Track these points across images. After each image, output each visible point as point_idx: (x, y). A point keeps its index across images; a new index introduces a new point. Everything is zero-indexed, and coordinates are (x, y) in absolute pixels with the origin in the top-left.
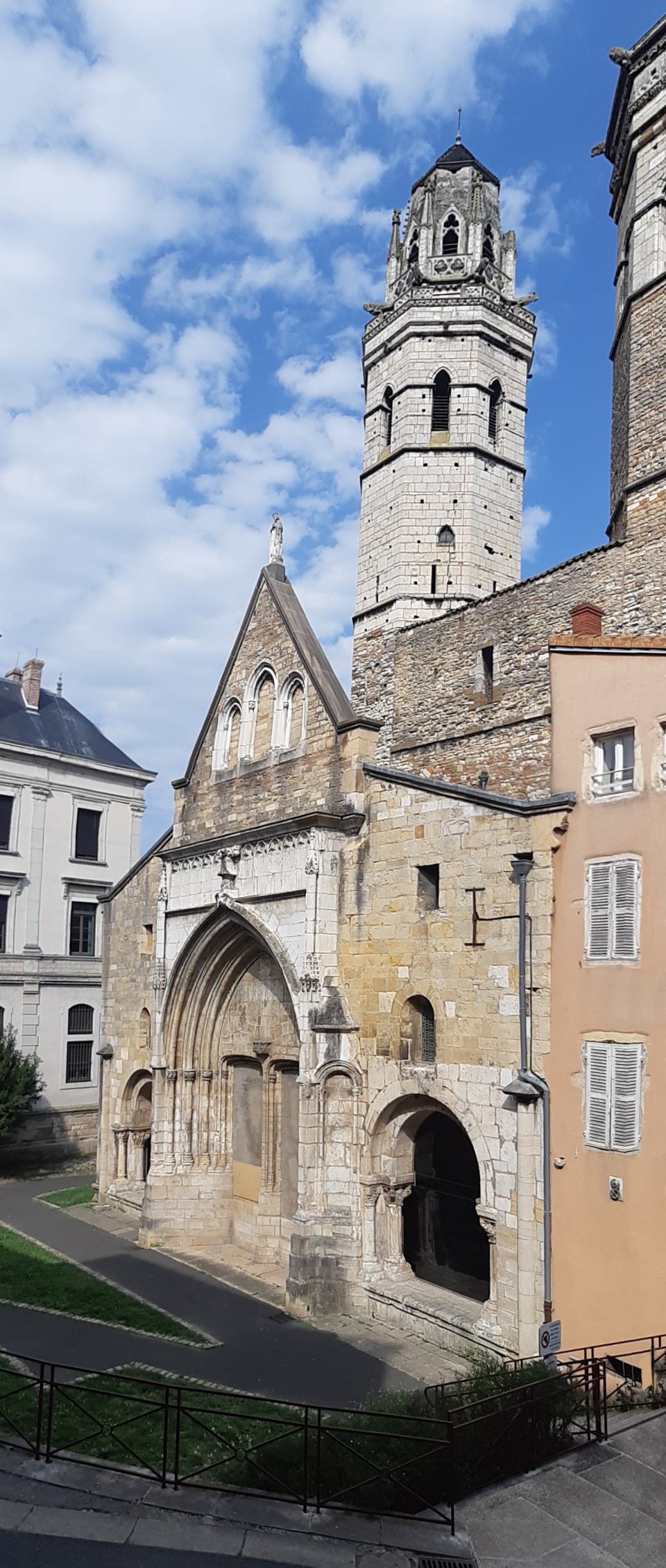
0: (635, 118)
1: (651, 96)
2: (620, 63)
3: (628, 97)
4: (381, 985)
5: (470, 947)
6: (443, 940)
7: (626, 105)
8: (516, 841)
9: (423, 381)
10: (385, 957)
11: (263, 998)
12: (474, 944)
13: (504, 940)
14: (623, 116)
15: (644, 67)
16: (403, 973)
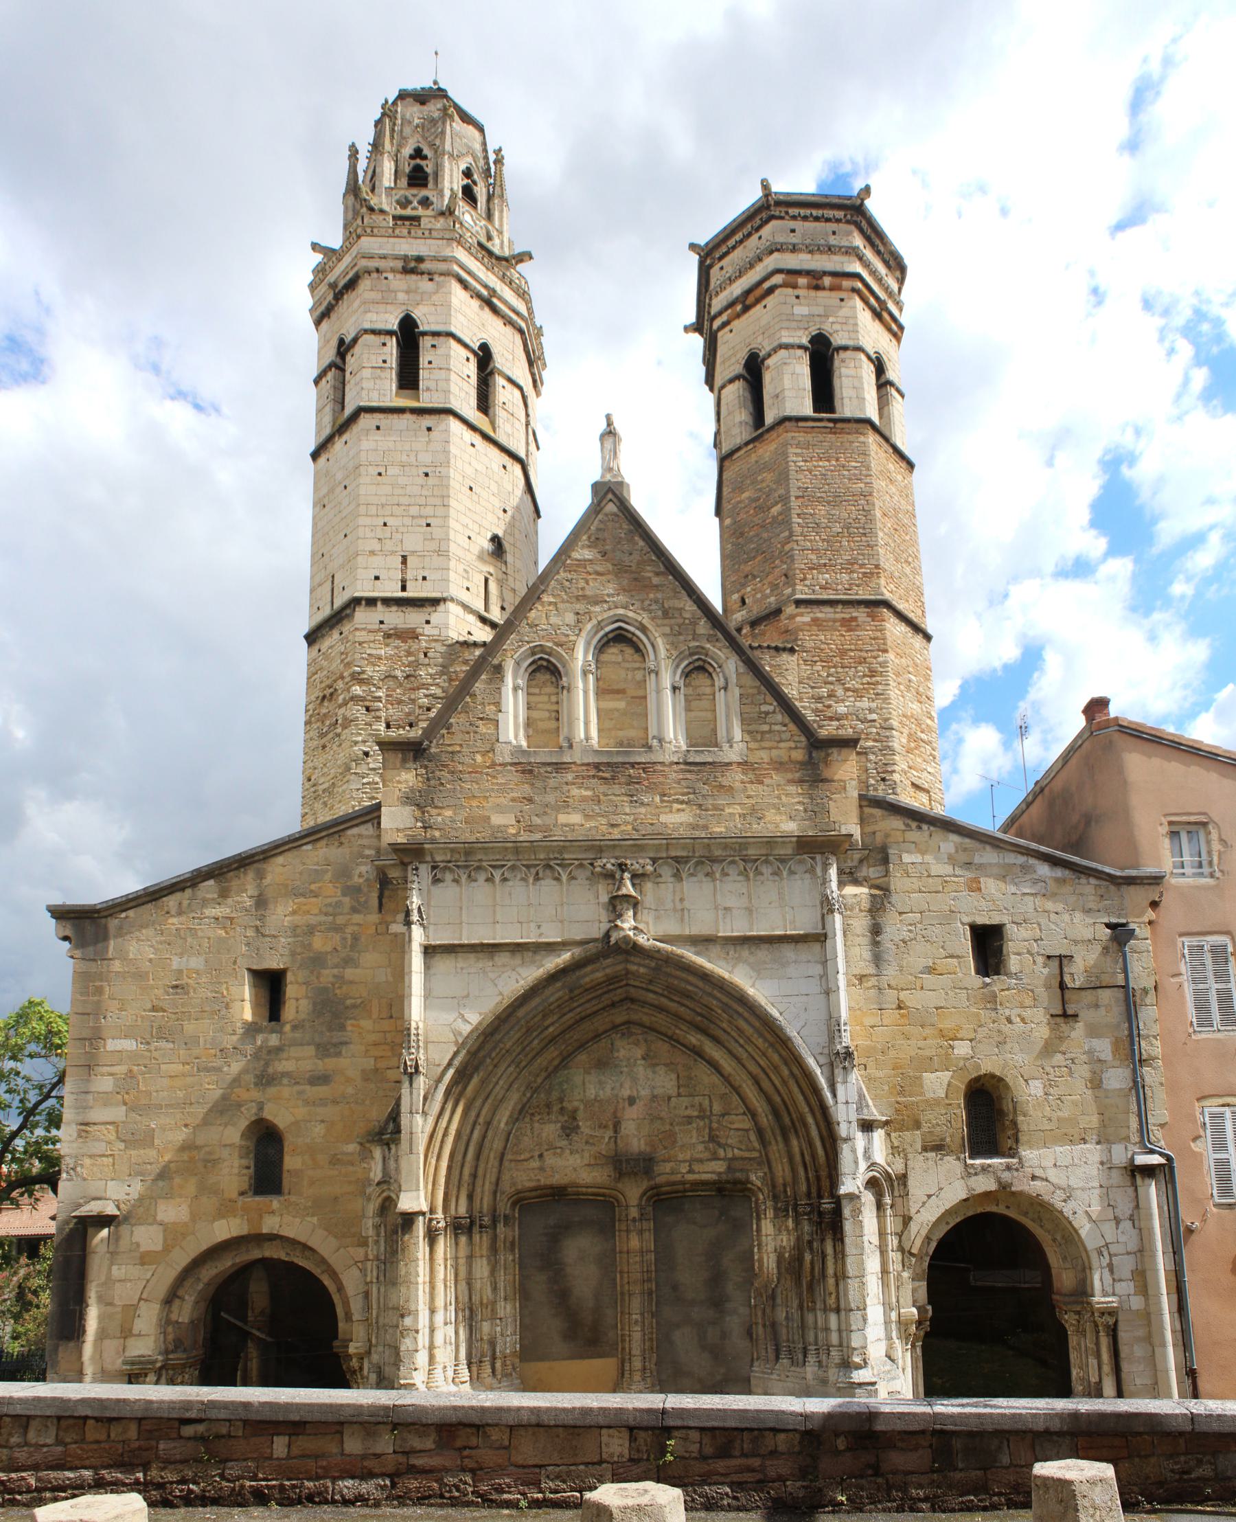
4: (928, 1064)
5: (1059, 1020)
6: (1019, 1011)
8: (1107, 911)
9: (468, 341)
10: (928, 1031)
11: (626, 1093)
12: (1065, 1015)
13: (1102, 1011)
15: (782, 218)
16: (962, 1049)
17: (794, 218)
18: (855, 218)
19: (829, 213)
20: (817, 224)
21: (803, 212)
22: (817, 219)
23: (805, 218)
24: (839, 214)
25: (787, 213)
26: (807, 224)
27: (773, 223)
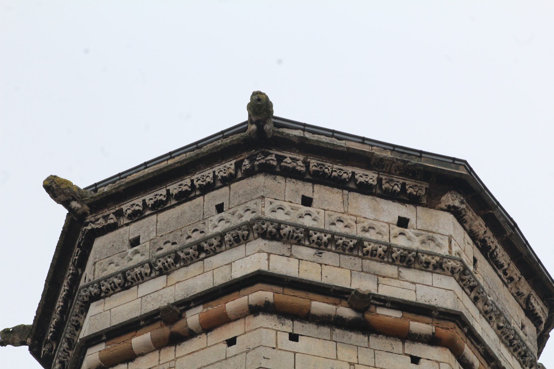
0: (94, 308)
1: (127, 281)
2: (66, 204)
3: (82, 263)
7: (76, 278)
14: (70, 296)
17: (136, 216)
18: (260, 160)
19: (206, 175)
20: (186, 206)
21: (149, 198)
22: (183, 197)
23: (159, 207)
24: (227, 167)
25: (119, 214)
26: (163, 216)
27: (99, 243)
